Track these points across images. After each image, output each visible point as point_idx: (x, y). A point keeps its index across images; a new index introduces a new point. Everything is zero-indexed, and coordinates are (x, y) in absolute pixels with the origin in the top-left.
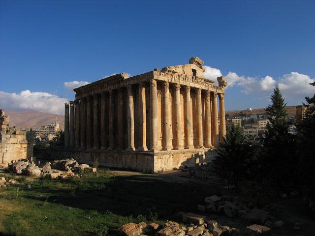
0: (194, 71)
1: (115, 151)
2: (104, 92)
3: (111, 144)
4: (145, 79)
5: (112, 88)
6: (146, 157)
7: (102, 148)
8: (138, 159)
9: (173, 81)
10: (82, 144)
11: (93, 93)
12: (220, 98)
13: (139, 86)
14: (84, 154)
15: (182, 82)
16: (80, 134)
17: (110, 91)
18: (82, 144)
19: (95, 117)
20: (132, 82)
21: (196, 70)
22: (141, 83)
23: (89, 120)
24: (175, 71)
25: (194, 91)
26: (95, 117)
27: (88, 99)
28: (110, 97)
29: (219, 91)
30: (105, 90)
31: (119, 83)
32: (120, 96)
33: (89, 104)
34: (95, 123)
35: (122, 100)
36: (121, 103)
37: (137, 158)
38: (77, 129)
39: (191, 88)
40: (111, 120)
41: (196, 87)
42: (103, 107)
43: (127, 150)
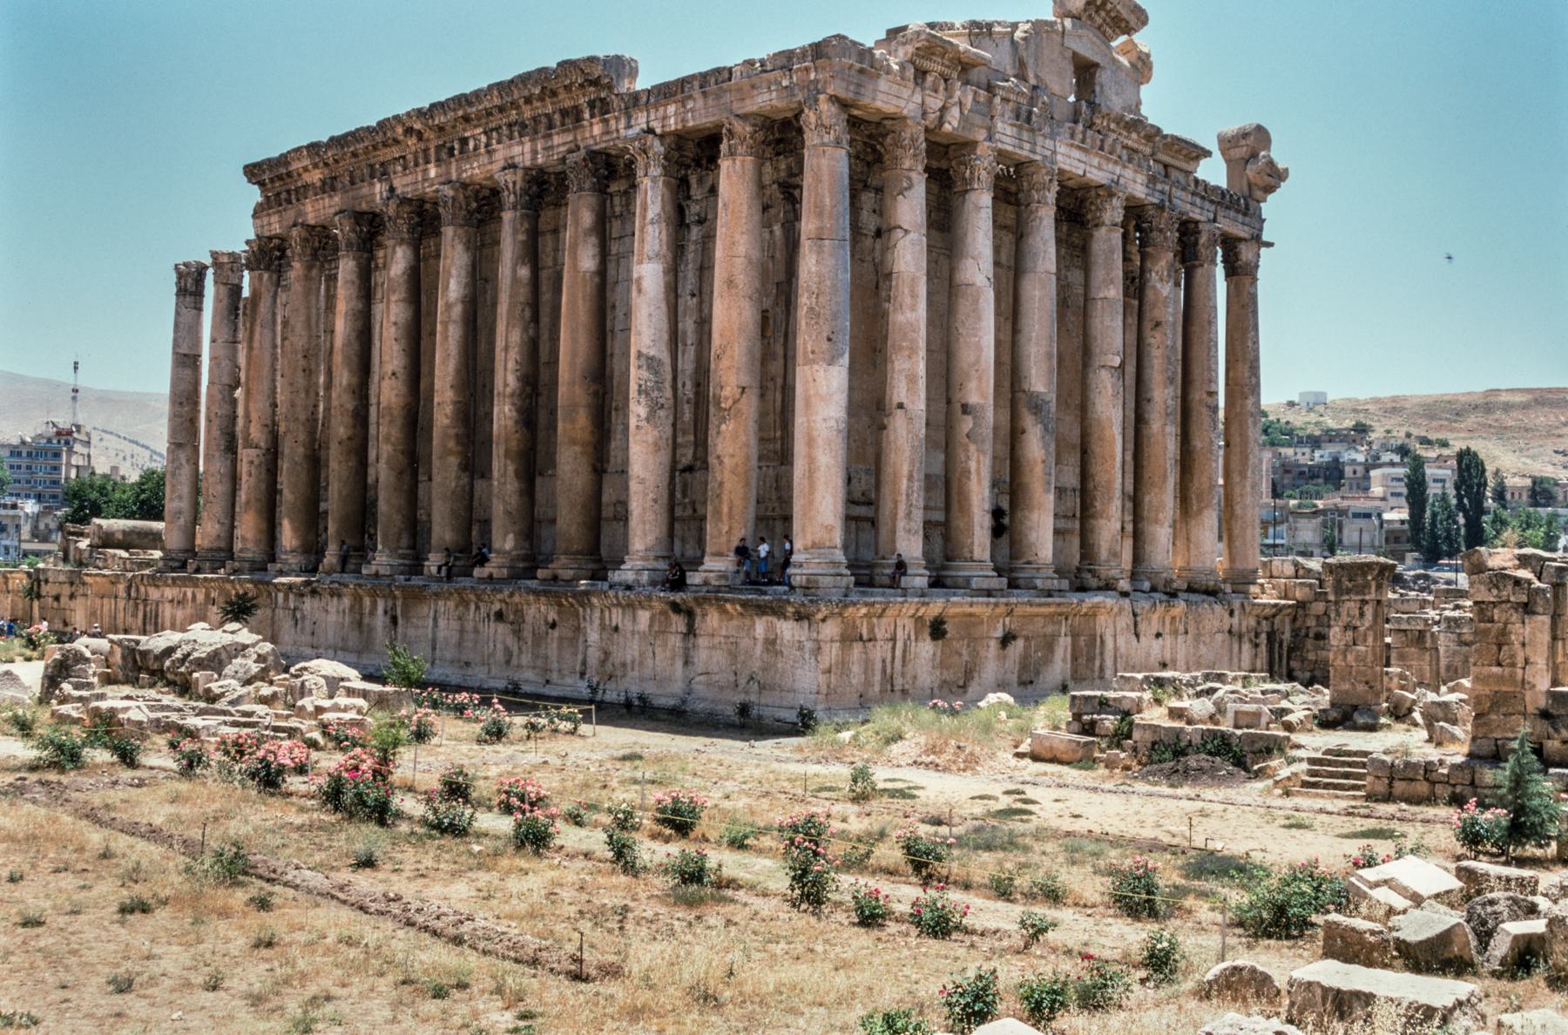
0: (1085, 72)
2: (465, 186)
3: (505, 542)
5: (522, 152)
6: (760, 626)
8: (702, 642)
9: (952, 123)
10: (288, 536)
12: (1241, 273)
13: (724, 147)
18: (288, 536)
19: (390, 355)
20: (671, 118)
21: (1096, 65)
25: (1077, 207)
26: (390, 355)
27: (342, 231)
28: (507, 216)
29: (1230, 224)
30: (474, 170)
31: (573, 116)
32: (580, 213)
33: (346, 267)
34: (388, 391)
35: (593, 240)
36: (588, 261)
37: (691, 632)
38: (257, 433)
39: (1063, 178)
40: (507, 376)
41: (1098, 176)
42: (453, 289)
43: (615, 576)
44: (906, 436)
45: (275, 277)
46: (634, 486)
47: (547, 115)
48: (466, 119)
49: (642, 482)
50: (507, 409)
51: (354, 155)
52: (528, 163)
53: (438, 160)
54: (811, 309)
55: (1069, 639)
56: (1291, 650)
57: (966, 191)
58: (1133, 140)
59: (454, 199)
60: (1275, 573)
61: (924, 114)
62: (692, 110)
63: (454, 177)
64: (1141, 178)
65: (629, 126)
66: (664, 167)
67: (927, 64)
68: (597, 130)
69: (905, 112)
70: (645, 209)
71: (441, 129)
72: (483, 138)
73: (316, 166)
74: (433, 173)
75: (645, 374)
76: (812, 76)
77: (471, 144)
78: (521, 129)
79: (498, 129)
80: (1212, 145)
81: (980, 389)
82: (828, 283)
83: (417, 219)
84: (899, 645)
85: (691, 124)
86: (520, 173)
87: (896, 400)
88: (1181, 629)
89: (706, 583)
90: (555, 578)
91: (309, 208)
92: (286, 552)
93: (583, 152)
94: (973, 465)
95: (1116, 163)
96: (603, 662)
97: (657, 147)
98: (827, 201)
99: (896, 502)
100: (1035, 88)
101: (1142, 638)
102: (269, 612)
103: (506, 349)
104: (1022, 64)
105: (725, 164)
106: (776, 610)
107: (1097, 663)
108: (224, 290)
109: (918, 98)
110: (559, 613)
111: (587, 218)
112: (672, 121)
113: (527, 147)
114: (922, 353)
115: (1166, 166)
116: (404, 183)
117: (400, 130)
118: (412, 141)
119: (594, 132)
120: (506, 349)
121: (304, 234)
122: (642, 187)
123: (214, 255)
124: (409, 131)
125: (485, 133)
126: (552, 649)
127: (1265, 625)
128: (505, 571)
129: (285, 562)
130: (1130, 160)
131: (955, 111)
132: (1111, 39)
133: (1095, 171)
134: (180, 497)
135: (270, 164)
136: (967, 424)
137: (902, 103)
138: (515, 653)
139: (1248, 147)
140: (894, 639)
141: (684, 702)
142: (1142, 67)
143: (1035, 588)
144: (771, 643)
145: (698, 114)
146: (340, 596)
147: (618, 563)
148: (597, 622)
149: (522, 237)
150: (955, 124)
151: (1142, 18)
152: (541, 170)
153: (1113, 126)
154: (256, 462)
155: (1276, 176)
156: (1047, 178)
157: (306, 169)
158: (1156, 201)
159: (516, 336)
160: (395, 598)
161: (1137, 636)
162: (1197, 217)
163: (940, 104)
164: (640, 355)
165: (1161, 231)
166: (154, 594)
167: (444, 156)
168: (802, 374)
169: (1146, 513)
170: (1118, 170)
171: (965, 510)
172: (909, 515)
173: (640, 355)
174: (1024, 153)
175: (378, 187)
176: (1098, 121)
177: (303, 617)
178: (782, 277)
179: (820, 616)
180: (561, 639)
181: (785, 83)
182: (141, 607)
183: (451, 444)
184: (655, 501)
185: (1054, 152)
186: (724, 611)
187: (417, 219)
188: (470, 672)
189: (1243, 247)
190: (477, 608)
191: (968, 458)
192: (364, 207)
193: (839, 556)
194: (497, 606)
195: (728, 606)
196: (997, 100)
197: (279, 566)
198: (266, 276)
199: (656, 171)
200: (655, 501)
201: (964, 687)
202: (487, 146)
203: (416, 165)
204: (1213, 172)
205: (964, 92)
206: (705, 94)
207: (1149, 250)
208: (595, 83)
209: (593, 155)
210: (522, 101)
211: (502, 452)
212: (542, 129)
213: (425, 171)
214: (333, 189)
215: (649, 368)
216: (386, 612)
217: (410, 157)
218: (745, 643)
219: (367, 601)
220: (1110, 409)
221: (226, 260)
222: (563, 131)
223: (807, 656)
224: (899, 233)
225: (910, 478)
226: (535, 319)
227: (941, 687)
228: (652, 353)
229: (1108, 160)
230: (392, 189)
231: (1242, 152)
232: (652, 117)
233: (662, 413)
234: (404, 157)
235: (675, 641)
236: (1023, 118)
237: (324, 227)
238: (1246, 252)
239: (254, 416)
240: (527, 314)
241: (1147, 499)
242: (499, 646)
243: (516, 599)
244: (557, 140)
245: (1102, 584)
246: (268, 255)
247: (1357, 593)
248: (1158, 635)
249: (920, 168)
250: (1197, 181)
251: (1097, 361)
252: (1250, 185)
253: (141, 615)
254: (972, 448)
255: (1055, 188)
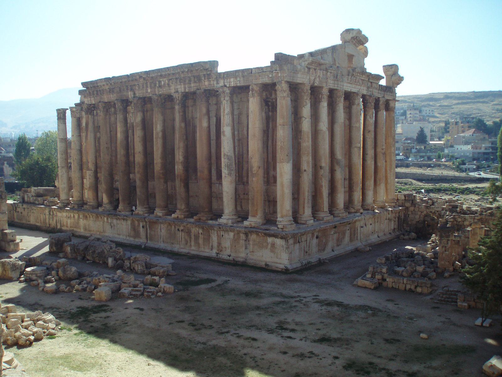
1: (192, 220)
2: (160, 95)
4: (266, 80)
5: (181, 88)
6: (270, 240)
7: (159, 212)
8: (251, 243)
10: (105, 200)
11: (130, 95)
14: (115, 221)
15: (331, 84)
16: (96, 178)
17: (176, 96)
19: (138, 147)
20: (233, 82)
22: (255, 88)
23: (121, 152)
24: (322, 61)
27: (119, 105)
28: (177, 107)
29: (387, 97)
30: (164, 91)
34: (139, 158)
35: (206, 117)
37: (247, 240)
38: (91, 166)
40: (179, 156)
41: (354, 90)
44: (306, 179)
45: (93, 117)
46: (225, 194)
47: (189, 77)
48: (161, 76)
49: (227, 193)
50: (180, 167)
51: (121, 82)
52: (183, 91)
53: (151, 88)
54: (281, 147)
55: (349, 231)
56: (404, 221)
57: (320, 102)
58: (364, 77)
59: (157, 100)
60: (399, 199)
61: (310, 81)
62: (238, 80)
63: (157, 93)
64: (365, 88)
65: (218, 83)
66: (230, 97)
67: (310, 66)
68: (207, 83)
69: (305, 82)
70: (224, 110)
71: (152, 77)
72: (167, 81)
73: (107, 84)
74: (149, 91)
75: (226, 160)
76: (279, 75)
77: (163, 83)
78: (182, 81)
79: (171, 79)
80: (383, 74)
81: (325, 162)
82: (287, 139)
83: (143, 103)
84: (308, 242)
85: (239, 85)
86: (180, 94)
87: (304, 169)
88: (377, 221)
89: (250, 225)
90: (200, 219)
91: (105, 97)
92: (105, 204)
93: (203, 90)
94: (323, 184)
95: (359, 85)
96: (218, 246)
97: (227, 91)
98: (285, 114)
99: (304, 199)
100: (338, 67)
101: (367, 226)
102: (102, 223)
103: (179, 148)
104: (335, 60)
105: (251, 100)
106: (275, 236)
107: (356, 236)
108: (75, 119)
109: (308, 78)
110: (203, 231)
111: (204, 110)
112: (232, 83)
113: (183, 86)
114: (311, 154)
115: (371, 83)
116: (139, 94)
117: (138, 77)
118: (142, 80)
119: (206, 84)
120: (179, 148)
121: (104, 105)
122: (223, 103)
123: (71, 108)
124: (141, 77)
125: (167, 80)
126: (201, 241)
127: (397, 215)
128: (183, 216)
129: (105, 207)
130: (363, 83)
131: (318, 79)
132: (357, 47)
133: (353, 89)
134: (64, 183)
135: (91, 82)
136: (322, 172)
137: (304, 80)
138: (189, 241)
139: (394, 74)
140: (306, 241)
141: (246, 259)
142: (366, 54)
143: (340, 217)
144: (273, 245)
145: (240, 82)
146: (127, 220)
147: (220, 216)
148: (216, 234)
149: (181, 114)
150: (318, 83)
151: (366, 40)
152: (187, 93)
153: (358, 75)
154: (92, 174)
155: (401, 79)
156: (341, 94)
157: (104, 85)
158: (369, 94)
159: (182, 145)
160: (146, 222)
161: (366, 225)
162: (379, 96)
163: (314, 78)
164: (225, 155)
165: (370, 103)
166: (59, 214)
167: (153, 85)
168: (278, 165)
169: (366, 188)
170: (359, 87)
171: (322, 197)
172: (308, 202)
173: (225, 155)
174: (336, 88)
175: (130, 93)
176: (354, 74)
177: (114, 226)
178: (265, 129)
179: (288, 238)
180: (204, 239)
181: (270, 76)
182: (55, 218)
183: (161, 176)
184: (232, 198)
185: (343, 86)
186: (258, 235)
187: (143, 103)
188: (174, 246)
189: (390, 102)
190: (175, 227)
191: (322, 182)
192: (125, 98)
193: (291, 218)
194: (182, 228)
195: (260, 234)
196: (329, 73)
197: (103, 208)
198: (90, 116)
199: (227, 98)
200: (232, 198)
201: (324, 250)
202: (168, 84)
203: (143, 87)
204: (383, 82)
205: (320, 72)
206: (243, 77)
207: (367, 109)
208: (207, 70)
209: (205, 90)
210: (181, 73)
211: (179, 180)
212: (187, 81)
213: (147, 90)
214: (113, 92)
215: (228, 159)
216: (143, 227)
217: (141, 85)
218: (265, 244)
219: (136, 222)
220: (358, 161)
221: (74, 110)
222: (195, 82)
223: (285, 249)
224: (304, 119)
225: (308, 192)
226: (187, 139)
227: (318, 251)
228: (229, 154)
229: (357, 85)
230: (134, 94)
231: (390, 73)
232: (226, 81)
233: (233, 172)
234: (138, 85)
235: (242, 242)
236: (336, 77)
237: (110, 102)
238: (391, 104)
239: (90, 160)
240: (185, 137)
241: (366, 183)
242: (183, 239)
243: (188, 226)
244: (192, 85)
245: (355, 211)
246: (91, 109)
247: (447, 238)
248: (371, 224)
249: (309, 98)
250: (379, 85)
251: (353, 146)
252: (393, 83)
253: (55, 220)
254: (323, 179)
255: (343, 96)
